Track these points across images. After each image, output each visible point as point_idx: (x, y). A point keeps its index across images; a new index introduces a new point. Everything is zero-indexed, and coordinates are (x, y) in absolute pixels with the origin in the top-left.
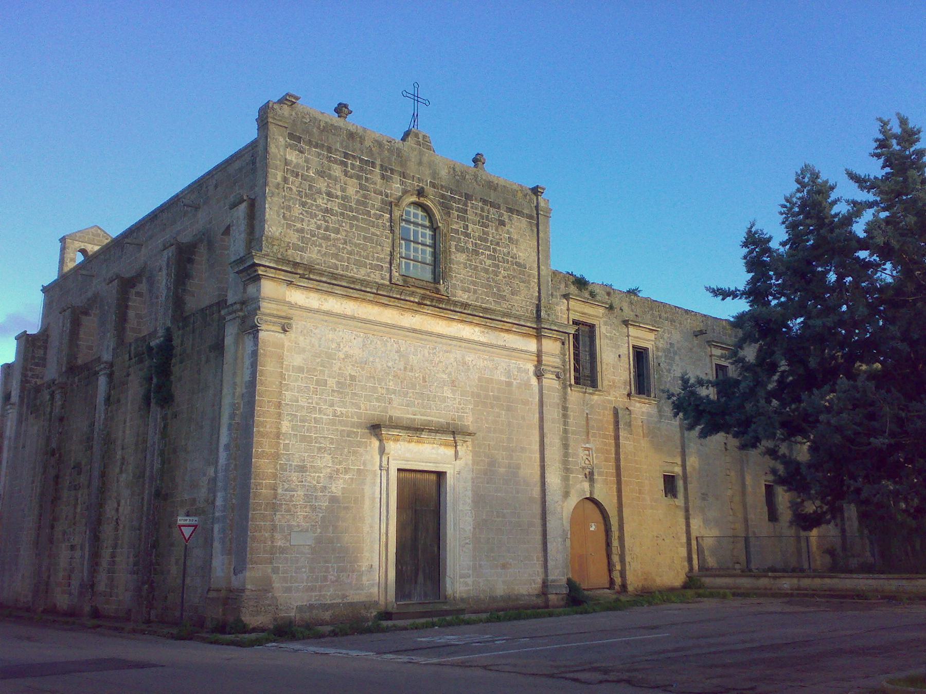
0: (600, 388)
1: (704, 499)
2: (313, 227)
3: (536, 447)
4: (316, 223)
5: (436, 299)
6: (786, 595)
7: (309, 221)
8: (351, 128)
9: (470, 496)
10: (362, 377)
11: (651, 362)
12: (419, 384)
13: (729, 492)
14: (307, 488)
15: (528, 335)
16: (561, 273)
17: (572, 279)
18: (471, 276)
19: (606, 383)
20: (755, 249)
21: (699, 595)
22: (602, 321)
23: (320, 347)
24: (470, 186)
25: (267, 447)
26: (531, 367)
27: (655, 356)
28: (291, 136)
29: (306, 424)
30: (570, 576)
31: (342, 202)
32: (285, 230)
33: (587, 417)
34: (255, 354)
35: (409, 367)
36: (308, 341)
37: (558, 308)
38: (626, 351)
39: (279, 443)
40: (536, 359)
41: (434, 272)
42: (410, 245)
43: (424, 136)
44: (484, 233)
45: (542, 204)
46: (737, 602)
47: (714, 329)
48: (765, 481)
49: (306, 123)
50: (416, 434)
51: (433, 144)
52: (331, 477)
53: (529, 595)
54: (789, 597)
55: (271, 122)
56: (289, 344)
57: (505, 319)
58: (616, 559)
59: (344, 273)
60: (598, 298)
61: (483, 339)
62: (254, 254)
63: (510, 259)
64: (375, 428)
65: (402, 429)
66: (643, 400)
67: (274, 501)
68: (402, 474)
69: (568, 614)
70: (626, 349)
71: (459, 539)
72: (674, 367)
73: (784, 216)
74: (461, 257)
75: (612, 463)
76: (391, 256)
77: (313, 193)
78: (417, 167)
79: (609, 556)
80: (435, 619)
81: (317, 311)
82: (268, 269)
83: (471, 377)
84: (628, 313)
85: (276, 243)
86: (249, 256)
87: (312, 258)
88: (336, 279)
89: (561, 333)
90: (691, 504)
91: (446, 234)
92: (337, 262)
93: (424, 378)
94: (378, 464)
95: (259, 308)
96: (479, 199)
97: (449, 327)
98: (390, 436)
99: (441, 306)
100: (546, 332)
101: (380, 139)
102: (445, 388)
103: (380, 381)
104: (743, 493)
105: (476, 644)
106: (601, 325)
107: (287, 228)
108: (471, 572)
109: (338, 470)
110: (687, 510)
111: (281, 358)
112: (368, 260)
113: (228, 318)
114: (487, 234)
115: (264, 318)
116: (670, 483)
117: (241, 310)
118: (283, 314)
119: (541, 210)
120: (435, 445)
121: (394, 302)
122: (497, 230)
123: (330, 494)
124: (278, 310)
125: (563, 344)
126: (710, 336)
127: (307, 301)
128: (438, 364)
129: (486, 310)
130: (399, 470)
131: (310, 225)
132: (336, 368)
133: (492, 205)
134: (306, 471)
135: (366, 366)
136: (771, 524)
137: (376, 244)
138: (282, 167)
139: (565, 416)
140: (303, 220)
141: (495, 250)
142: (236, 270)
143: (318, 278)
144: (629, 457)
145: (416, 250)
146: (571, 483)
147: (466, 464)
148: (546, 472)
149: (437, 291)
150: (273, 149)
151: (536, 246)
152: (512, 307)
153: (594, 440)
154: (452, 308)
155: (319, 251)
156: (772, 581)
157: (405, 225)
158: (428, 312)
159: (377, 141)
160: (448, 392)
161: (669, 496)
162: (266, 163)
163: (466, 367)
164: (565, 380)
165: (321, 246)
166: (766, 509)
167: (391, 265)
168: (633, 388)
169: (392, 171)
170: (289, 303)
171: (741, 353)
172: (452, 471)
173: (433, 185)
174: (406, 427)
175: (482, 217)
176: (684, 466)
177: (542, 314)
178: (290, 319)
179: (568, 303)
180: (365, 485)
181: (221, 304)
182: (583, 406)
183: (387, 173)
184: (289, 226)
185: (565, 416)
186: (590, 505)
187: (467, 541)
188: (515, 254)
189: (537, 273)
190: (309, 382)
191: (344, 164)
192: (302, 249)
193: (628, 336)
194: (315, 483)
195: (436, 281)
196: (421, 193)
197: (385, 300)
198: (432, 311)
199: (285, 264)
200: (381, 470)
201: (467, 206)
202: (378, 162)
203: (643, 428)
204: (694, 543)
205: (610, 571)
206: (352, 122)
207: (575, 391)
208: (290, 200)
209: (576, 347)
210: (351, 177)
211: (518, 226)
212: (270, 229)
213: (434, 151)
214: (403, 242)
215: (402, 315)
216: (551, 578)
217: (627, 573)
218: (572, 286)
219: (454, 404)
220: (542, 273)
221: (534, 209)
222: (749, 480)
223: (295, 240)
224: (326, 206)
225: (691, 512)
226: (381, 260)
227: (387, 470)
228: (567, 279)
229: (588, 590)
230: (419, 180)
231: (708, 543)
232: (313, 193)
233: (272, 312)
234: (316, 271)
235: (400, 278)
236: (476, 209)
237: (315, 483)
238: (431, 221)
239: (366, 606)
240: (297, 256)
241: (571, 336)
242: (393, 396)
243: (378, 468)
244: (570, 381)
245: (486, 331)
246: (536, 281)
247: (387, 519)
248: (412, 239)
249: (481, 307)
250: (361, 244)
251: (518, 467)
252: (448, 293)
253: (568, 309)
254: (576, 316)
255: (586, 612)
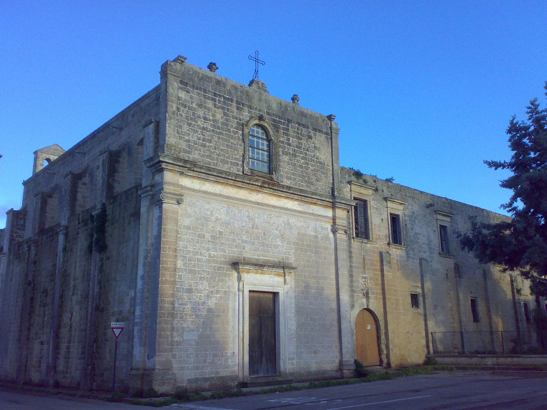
0: (371, 239)
1: (435, 309)
2: (195, 139)
3: (333, 276)
4: (197, 136)
5: (272, 184)
6: (490, 369)
7: (193, 135)
8: (218, 78)
9: (294, 307)
10: (227, 232)
11: (401, 224)
12: (262, 237)
13: (450, 305)
14: (193, 303)
15: (328, 207)
16: (346, 168)
17: (352, 172)
18: (292, 170)
19: (374, 236)
20: (516, 134)
21: (436, 369)
22: (371, 198)
23: (200, 213)
24: (290, 114)
25: (168, 277)
26: (329, 227)
27: (403, 220)
28: (182, 82)
29: (192, 262)
30: (356, 358)
31: (213, 123)
32: (178, 140)
33: (364, 258)
34: (160, 218)
35: (255, 226)
36: (193, 210)
37: (345, 190)
38: (386, 216)
39: (176, 275)
40: (332, 221)
41: (269, 167)
42: (255, 150)
43: (262, 83)
44: (299, 143)
45: (334, 126)
46: (461, 373)
47: (438, 203)
48: (471, 297)
49: (191, 74)
50: (260, 268)
51: (268, 89)
52: (208, 296)
53: (331, 370)
54: (492, 369)
55: (169, 73)
56: (182, 212)
57: (313, 197)
58: (383, 347)
59: (215, 167)
60: (369, 184)
61: (300, 209)
62: (159, 154)
63: (315, 159)
64: (235, 265)
65: (252, 265)
66: (397, 247)
67: (173, 311)
68: (252, 294)
69: (359, 383)
70: (386, 215)
71: (288, 335)
72: (415, 226)
73: (530, 114)
74: (286, 158)
75: (380, 287)
76: (243, 157)
77: (195, 117)
78: (258, 102)
79: (379, 345)
80: (276, 387)
81: (198, 191)
82: (168, 164)
83: (293, 232)
84: (386, 193)
85: (173, 148)
86: (156, 156)
87: (195, 158)
88: (210, 171)
89: (347, 205)
90: (427, 312)
91: (276, 143)
92: (210, 161)
93: (264, 234)
94: (237, 288)
95: (163, 189)
96: (296, 122)
97: (279, 201)
98: (244, 270)
99: (274, 188)
100: (338, 205)
101: (236, 85)
102: (277, 239)
103: (237, 235)
104: (458, 305)
105: (309, 404)
106: (371, 201)
107: (180, 139)
108: (295, 356)
109: (212, 291)
110: (425, 316)
111: (176, 220)
112: (229, 159)
113: (142, 196)
114: (301, 144)
115: (166, 195)
116: (414, 298)
117: (151, 190)
118: (178, 193)
119: (334, 130)
120: (272, 276)
121: (245, 185)
122: (307, 141)
123: (207, 307)
124: (174, 190)
125: (348, 212)
126: (436, 207)
127: (192, 185)
128: (273, 224)
129: (301, 191)
130: (250, 291)
131: (193, 137)
132: (210, 227)
133: (304, 126)
134: (192, 292)
135: (229, 226)
136: (475, 324)
137: (234, 150)
138: (176, 102)
139: (350, 257)
140: (189, 135)
141: (306, 154)
142: (148, 165)
143: (199, 170)
144: (390, 283)
145: (258, 154)
146: (355, 299)
147: (291, 288)
148: (340, 292)
149: (272, 179)
150: (170, 90)
151: (331, 152)
152: (317, 189)
153: (369, 272)
154: (281, 189)
155: (199, 154)
156: (480, 359)
157: (251, 138)
158: (266, 192)
159: (234, 86)
160: (279, 242)
161: (414, 306)
162: (166, 99)
163: (290, 226)
164: (350, 234)
165: (200, 150)
166: (471, 315)
167: (243, 162)
168: (391, 240)
169: (243, 105)
170: (182, 186)
171: (515, 204)
172: (283, 292)
173: (268, 114)
174: (254, 264)
175: (298, 134)
176: (423, 288)
177: (335, 193)
178: (182, 196)
179: (351, 187)
180: (229, 301)
181: (138, 187)
182: (361, 250)
183: (240, 106)
184: (181, 138)
185: (350, 257)
186: (367, 313)
187: (293, 336)
188: (318, 157)
189: (331, 168)
190: (194, 236)
191: (214, 100)
192: (189, 153)
193: (387, 207)
194: (198, 300)
195: (270, 172)
196: (261, 118)
197: (240, 184)
198: (269, 191)
199: (179, 161)
200: (239, 291)
201: (289, 127)
202: (235, 99)
203: (397, 264)
204: (430, 336)
205: (380, 355)
206: (219, 75)
207: (356, 241)
208: (181, 122)
209: (356, 214)
210: (219, 108)
211: (320, 139)
212: (169, 140)
213: (268, 93)
214: (250, 149)
215: (250, 194)
216: (344, 359)
217: (391, 355)
218: (353, 177)
219: (283, 249)
220: (335, 168)
221: (329, 129)
222: (461, 296)
223: (184, 147)
224: (203, 126)
225: (428, 317)
226: (237, 159)
227: (243, 291)
228: (350, 172)
229: (366, 367)
230: (260, 110)
231: (438, 336)
232: (195, 117)
233: (171, 191)
234: (198, 166)
235: (249, 171)
236: (294, 128)
237: (198, 300)
238: (267, 136)
239: (233, 378)
240: (185, 156)
241: (353, 207)
242: (245, 245)
243: (237, 290)
244: (353, 236)
245: (302, 204)
246: (331, 173)
247: (243, 323)
248: (256, 147)
249: (298, 189)
250: (225, 149)
251: (323, 289)
252: (278, 180)
253: (351, 191)
254: (356, 195)
255: (370, 381)
